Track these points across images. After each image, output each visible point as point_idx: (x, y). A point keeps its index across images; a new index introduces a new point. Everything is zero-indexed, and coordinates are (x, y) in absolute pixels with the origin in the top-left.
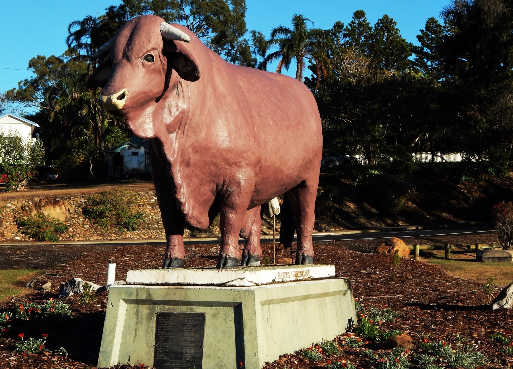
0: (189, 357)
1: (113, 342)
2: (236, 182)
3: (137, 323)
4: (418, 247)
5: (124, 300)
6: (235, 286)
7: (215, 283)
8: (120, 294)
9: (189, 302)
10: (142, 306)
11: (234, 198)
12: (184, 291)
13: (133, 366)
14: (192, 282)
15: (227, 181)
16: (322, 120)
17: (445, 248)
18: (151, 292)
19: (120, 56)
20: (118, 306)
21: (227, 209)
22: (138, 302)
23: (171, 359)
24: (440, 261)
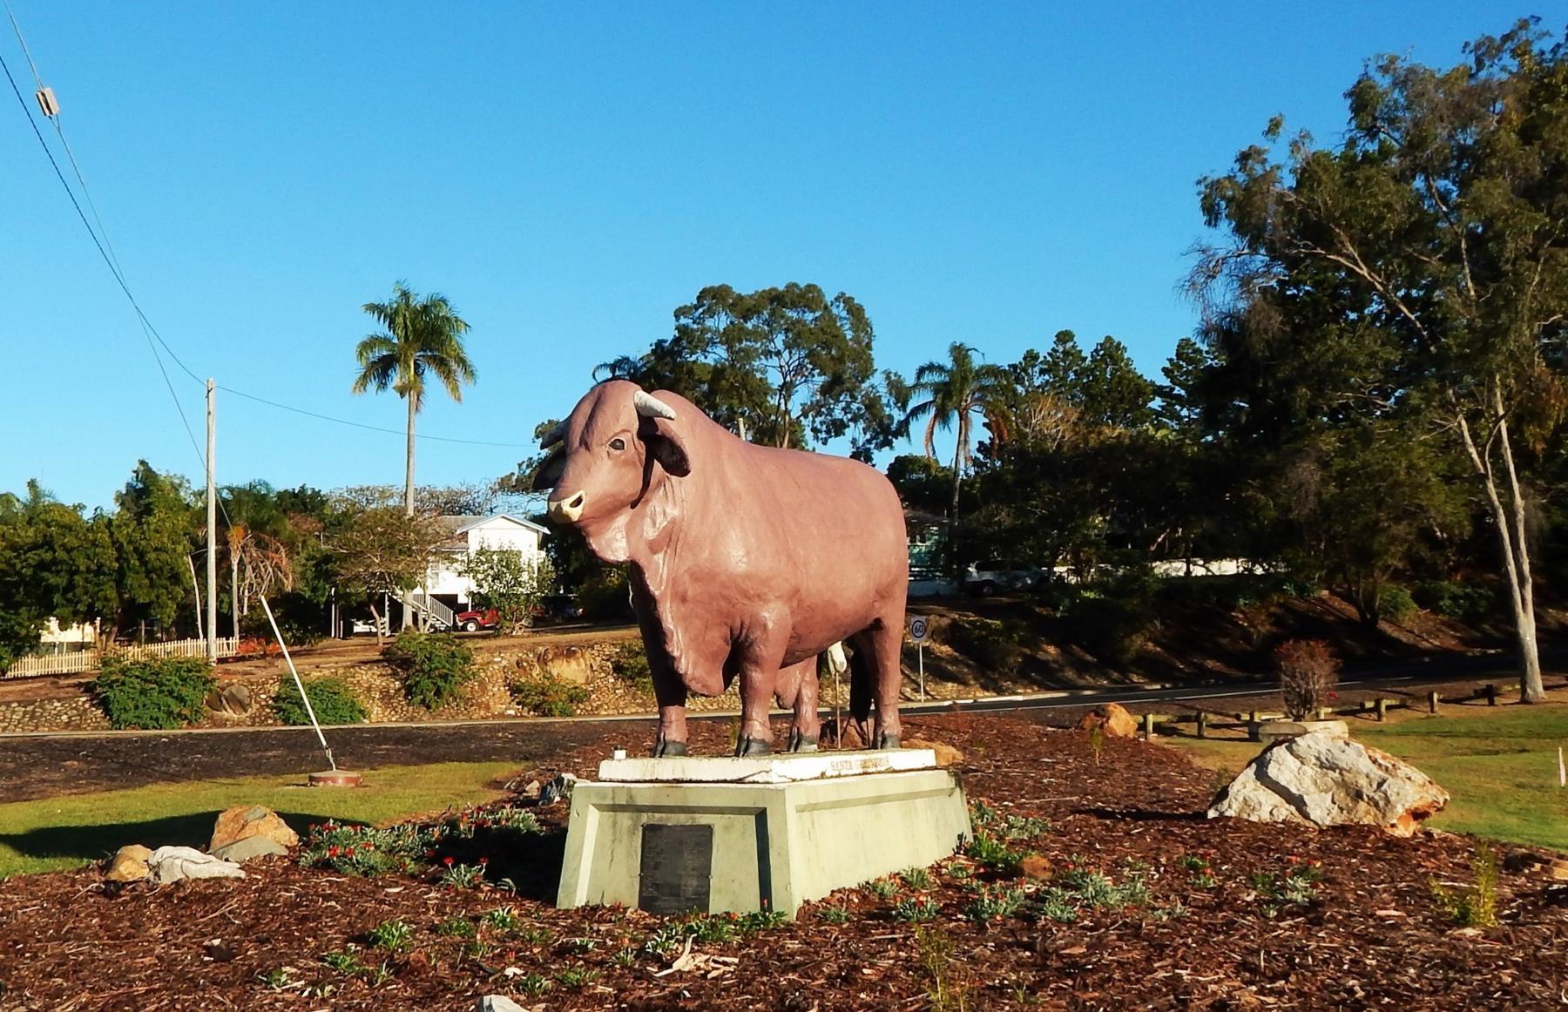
3: (613, 841)
4: (1151, 718)
5: (594, 805)
6: (758, 783)
7: (729, 779)
8: (589, 796)
9: (688, 807)
14: (694, 778)
15: (747, 623)
17: (1197, 719)
18: (634, 793)
19: (576, 443)
21: (748, 666)
22: (615, 808)
24: (1187, 740)
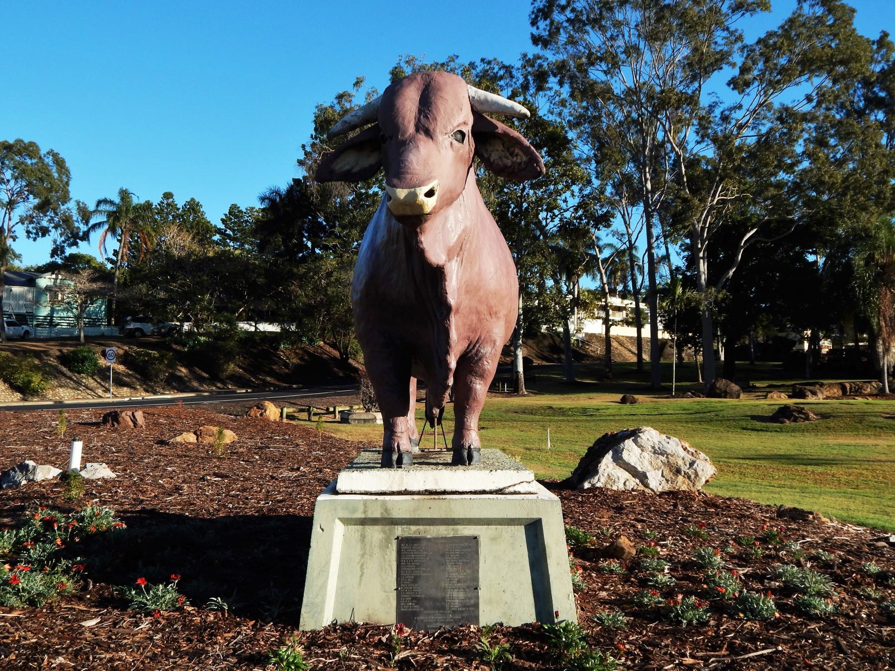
0: (456, 604)
1: (326, 590)
2: (491, 340)
3: (363, 556)
4: (285, 410)
5: (341, 520)
6: (519, 493)
7: (487, 489)
8: (335, 510)
9: (453, 519)
10: (371, 527)
11: (486, 363)
12: (445, 503)
13: (362, 624)
14: (449, 488)
15: (482, 338)
16: (518, 263)
17: (309, 411)
18: (389, 506)
19: (411, 129)
20: (332, 530)
21: (473, 379)
22: (364, 522)
23: (426, 609)
24: (302, 423)
